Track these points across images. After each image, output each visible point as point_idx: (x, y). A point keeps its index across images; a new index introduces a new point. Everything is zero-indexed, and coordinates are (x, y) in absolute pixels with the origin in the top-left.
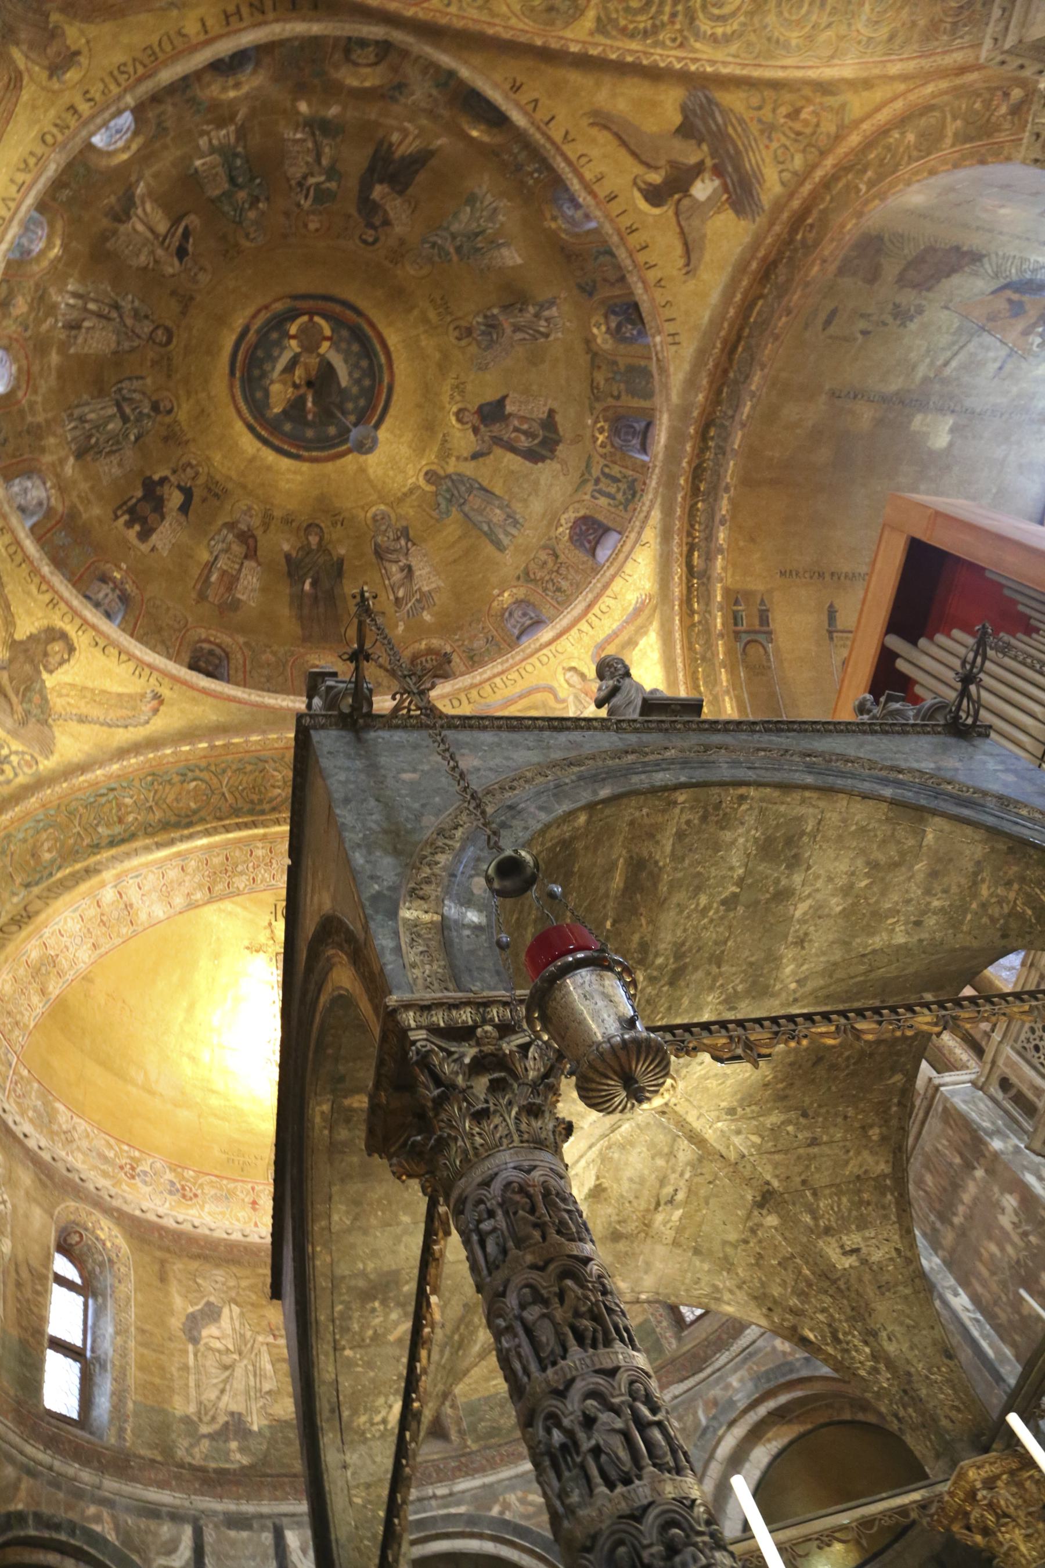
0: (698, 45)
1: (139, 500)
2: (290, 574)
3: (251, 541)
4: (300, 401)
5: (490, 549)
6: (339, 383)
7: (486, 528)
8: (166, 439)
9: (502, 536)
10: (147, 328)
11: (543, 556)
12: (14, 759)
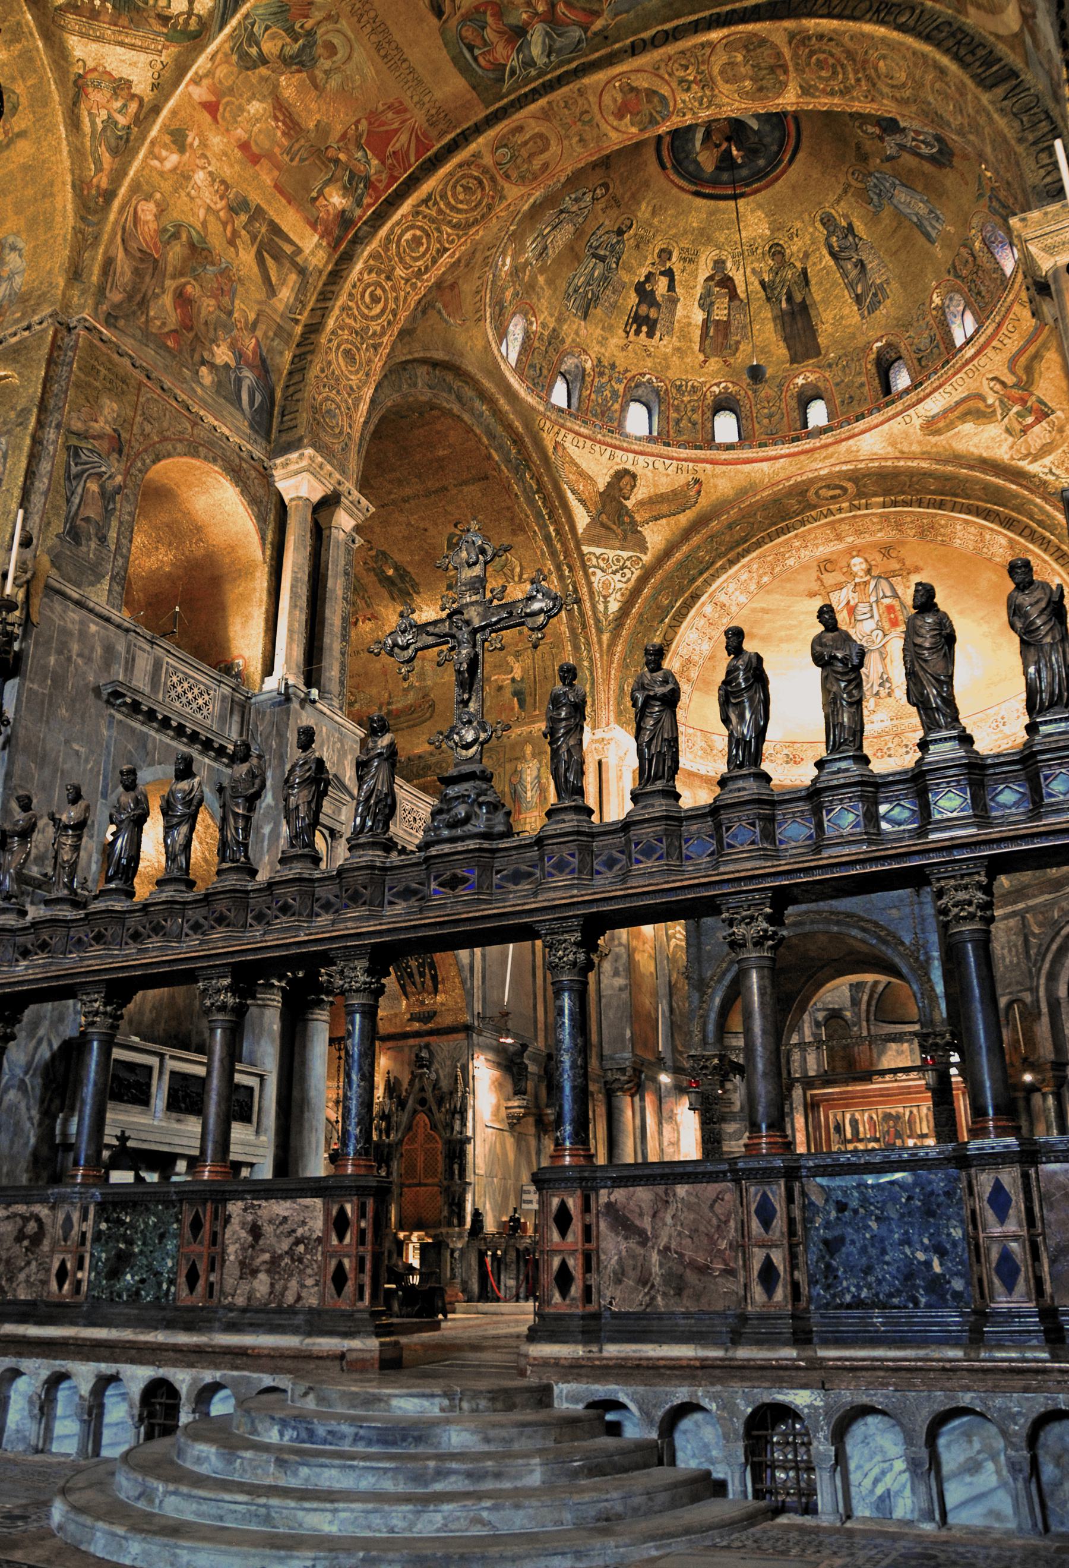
0: (885, 102)
1: (638, 305)
2: (768, 299)
3: (729, 283)
4: (728, 151)
5: (922, 240)
6: (751, 128)
7: (915, 219)
8: (637, 246)
9: (929, 229)
10: (588, 198)
11: (964, 251)
12: (628, 563)
